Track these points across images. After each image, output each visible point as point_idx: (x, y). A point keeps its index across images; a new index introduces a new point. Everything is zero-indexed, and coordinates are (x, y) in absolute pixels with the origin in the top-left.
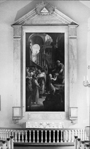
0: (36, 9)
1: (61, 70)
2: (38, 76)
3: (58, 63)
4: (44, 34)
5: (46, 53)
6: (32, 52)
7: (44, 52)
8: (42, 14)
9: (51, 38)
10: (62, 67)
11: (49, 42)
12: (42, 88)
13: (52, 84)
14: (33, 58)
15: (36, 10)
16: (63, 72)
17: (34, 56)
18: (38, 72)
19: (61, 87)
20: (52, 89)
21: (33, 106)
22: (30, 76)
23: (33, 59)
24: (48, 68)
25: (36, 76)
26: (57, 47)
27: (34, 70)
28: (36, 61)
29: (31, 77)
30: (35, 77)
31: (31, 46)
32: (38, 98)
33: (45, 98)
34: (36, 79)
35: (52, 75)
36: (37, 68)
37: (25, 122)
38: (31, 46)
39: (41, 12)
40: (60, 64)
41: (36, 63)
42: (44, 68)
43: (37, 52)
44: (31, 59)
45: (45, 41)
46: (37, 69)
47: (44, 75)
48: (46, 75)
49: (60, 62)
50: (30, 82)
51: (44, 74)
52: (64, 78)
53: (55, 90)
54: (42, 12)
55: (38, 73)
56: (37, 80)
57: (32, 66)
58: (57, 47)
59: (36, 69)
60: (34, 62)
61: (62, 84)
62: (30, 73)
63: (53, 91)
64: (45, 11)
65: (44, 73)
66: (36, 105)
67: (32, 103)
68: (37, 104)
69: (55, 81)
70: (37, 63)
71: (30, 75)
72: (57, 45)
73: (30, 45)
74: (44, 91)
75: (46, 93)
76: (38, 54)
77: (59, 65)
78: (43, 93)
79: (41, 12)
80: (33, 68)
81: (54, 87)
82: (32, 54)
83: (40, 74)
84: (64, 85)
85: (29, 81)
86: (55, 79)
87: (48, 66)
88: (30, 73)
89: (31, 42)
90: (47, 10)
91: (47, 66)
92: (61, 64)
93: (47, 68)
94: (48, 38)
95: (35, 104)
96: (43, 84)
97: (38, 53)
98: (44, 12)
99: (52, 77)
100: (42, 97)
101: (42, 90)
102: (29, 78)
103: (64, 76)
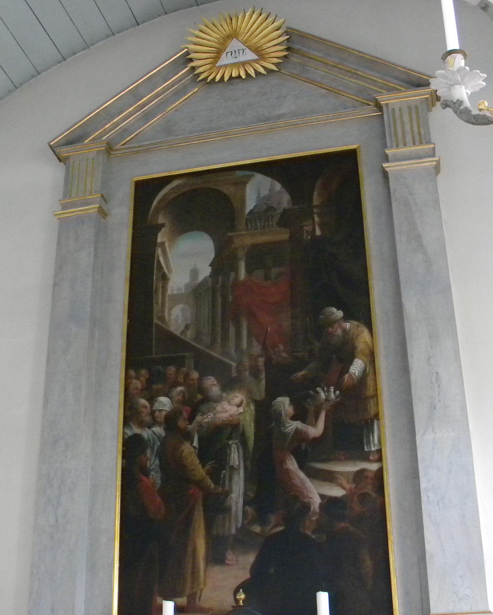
0: (188, 53)
1: (350, 362)
2: (199, 418)
3: (332, 323)
4: (239, 173)
5: (249, 271)
6: (165, 278)
7: (236, 270)
8: (223, 77)
9: (278, 186)
10: (354, 348)
11: (270, 209)
12: (227, 493)
13: (292, 464)
14: (170, 309)
15: (191, 60)
16: (364, 374)
17: (176, 299)
18: (201, 389)
19: (360, 474)
20: (296, 498)
22: (148, 419)
23: (173, 317)
24: (268, 363)
25: (191, 419)
26: (318, 232)
27: (181, 385)
28: (187, 327)
29: (159, 430)
30: (182, 423)
31: (163, 244)
32: (202, 565)
33: (251, 558)
34: (188, 437)
35: (292, 402)
36: (196, 369)
38: (163, 244)
40: (344, 331)
41: (189, 336)
42: (240, 363)
43: (194, 273)
44: (162, 318)
45: (247, 211)
46: (195, 375)
47: (241, 410)
48: (258, 404)
49: (347, 317)
51: (237, 400)
52: (377, 416)
53: (316, 501)
54: (226, 66)
55: (199, 397)
56: (196, 443)
57: (167, 362)
58: (318, 232)
59: (187, 375)
60: (178, 333)
61: (365, 457)
62: (152, 406)
63: (306, 507)
64: (242, 58)
65: (239, 397)
69: (315, 440)
70: (197, 338)
71: (152, 413)
72: (317, 219)
73: (159, 240)
74: (244, 513)
75: (257, 529)
76: (205, 281)
77: (339, 332)
78: (233, 531)
80: (172, 369)
81: (308, 482)
82: (164, 289)
83: (218, 400)
84: (374, 467)
85: (144, 451)
86: (314, 424)
87: (264, 347)
88: (152, 406)
89: (163, 225)
90: (247, 51)
91: (257, 349)
92: (348, 325)
93: (261, 361)
94: (265, 192)
96: (232, 468)
97: (201, 278)
98: (236, 61)
99: (294, 418)
100: (230, 556)
101: (228, 510)
102: (146, 433)
103: (372, 402)
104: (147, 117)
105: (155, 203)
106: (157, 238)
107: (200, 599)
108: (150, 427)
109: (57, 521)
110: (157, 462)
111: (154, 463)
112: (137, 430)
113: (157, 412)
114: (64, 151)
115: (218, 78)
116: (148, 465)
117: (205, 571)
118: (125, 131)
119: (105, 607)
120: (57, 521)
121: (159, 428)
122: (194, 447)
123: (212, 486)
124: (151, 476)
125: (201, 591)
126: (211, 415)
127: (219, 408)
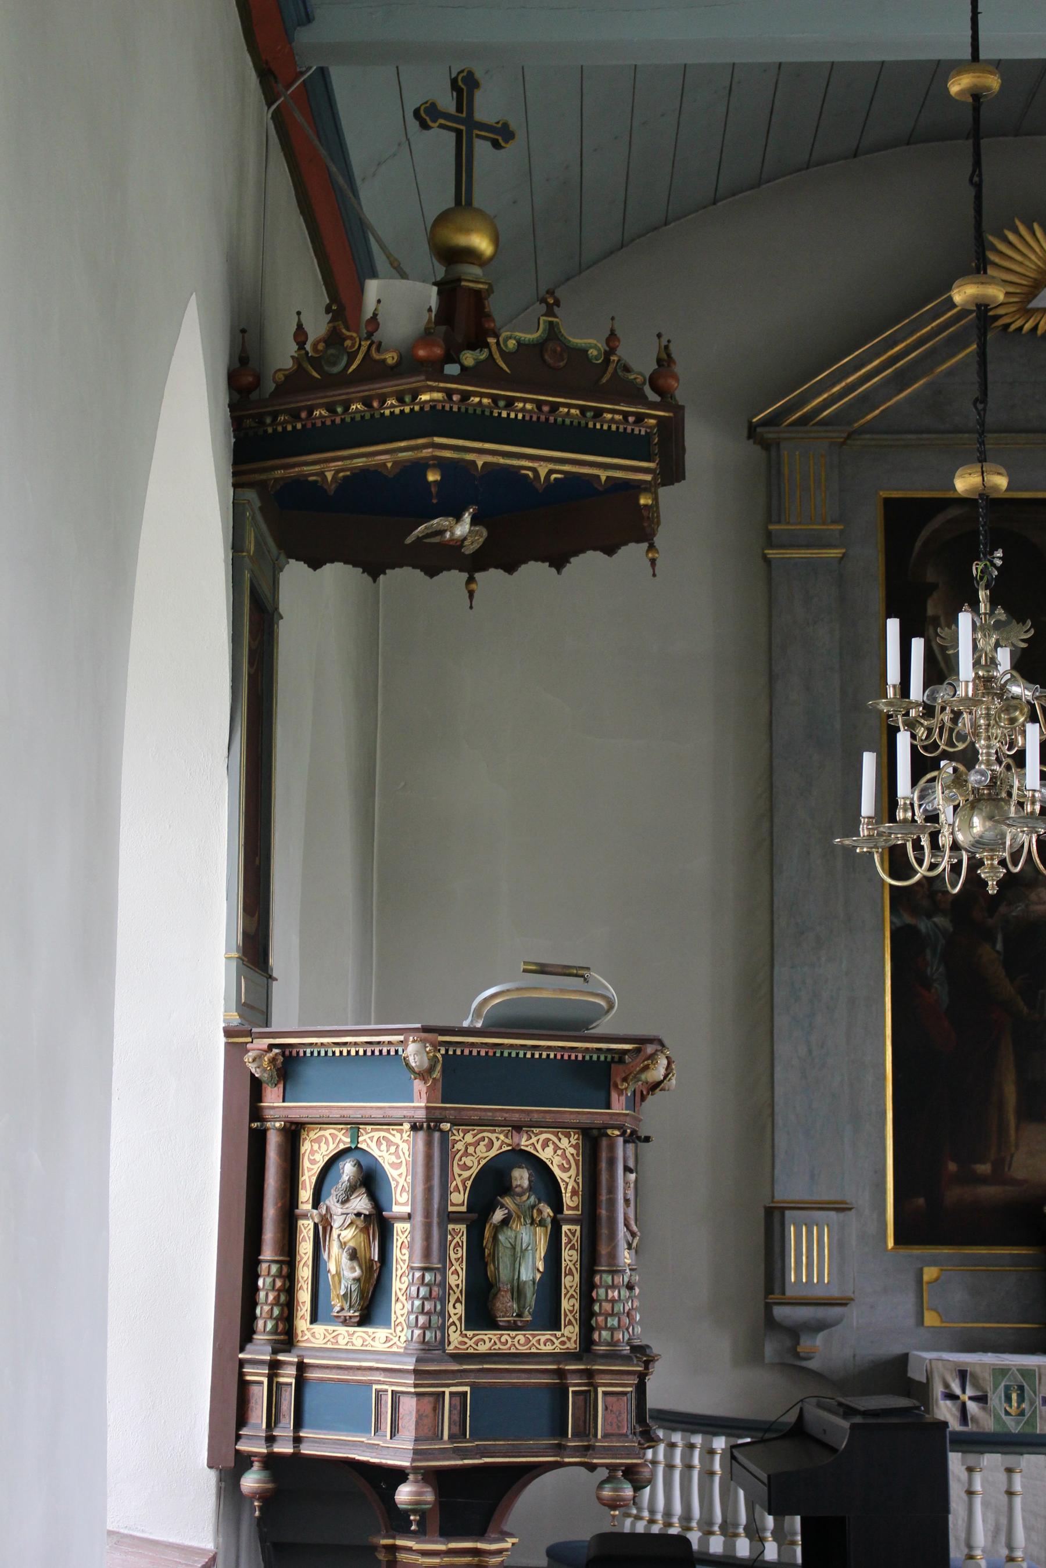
8: (1035, 328)
21: (954, 1194)
37: (897, 1350)
39: (1031, 306)
50: (935, 969)
56: (999, 946)
66: (988, 1192)
67: (952, 1167)
68: (998, 1177)
73: (930, 611)
79: (1031, 306)
95: (983, 1180)
102: (923, 926)
104: (901, 380)
105: (918, 544)
106: (925, 610)
107: (1009, 1168)
108: (929, 916)
109: (810, 1051)
110: (942, 969)
111: (937, 970)
112: (909, 920)
113: (940, 894)
114: (770, 433)
115: (1028, 326)
116: (929, 974)
117: (1017, 1129)
118: (866, 402)
119: (876, 1172)
120: (810, 1051)
121: (942, 919)
122: (998, 952)
123: (1026, 1010)
124: (933, 990)
125: (1012, 1156)
126: (1021, 907)
127: (1033, 896)
